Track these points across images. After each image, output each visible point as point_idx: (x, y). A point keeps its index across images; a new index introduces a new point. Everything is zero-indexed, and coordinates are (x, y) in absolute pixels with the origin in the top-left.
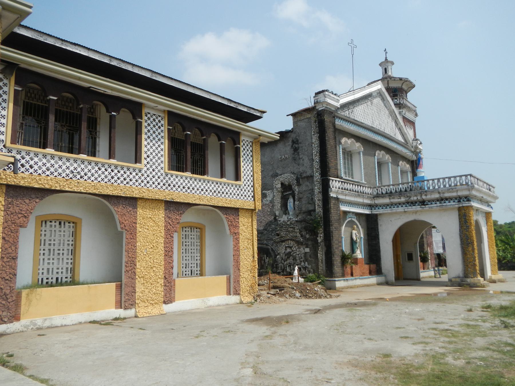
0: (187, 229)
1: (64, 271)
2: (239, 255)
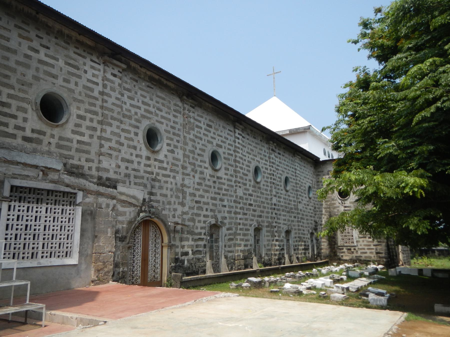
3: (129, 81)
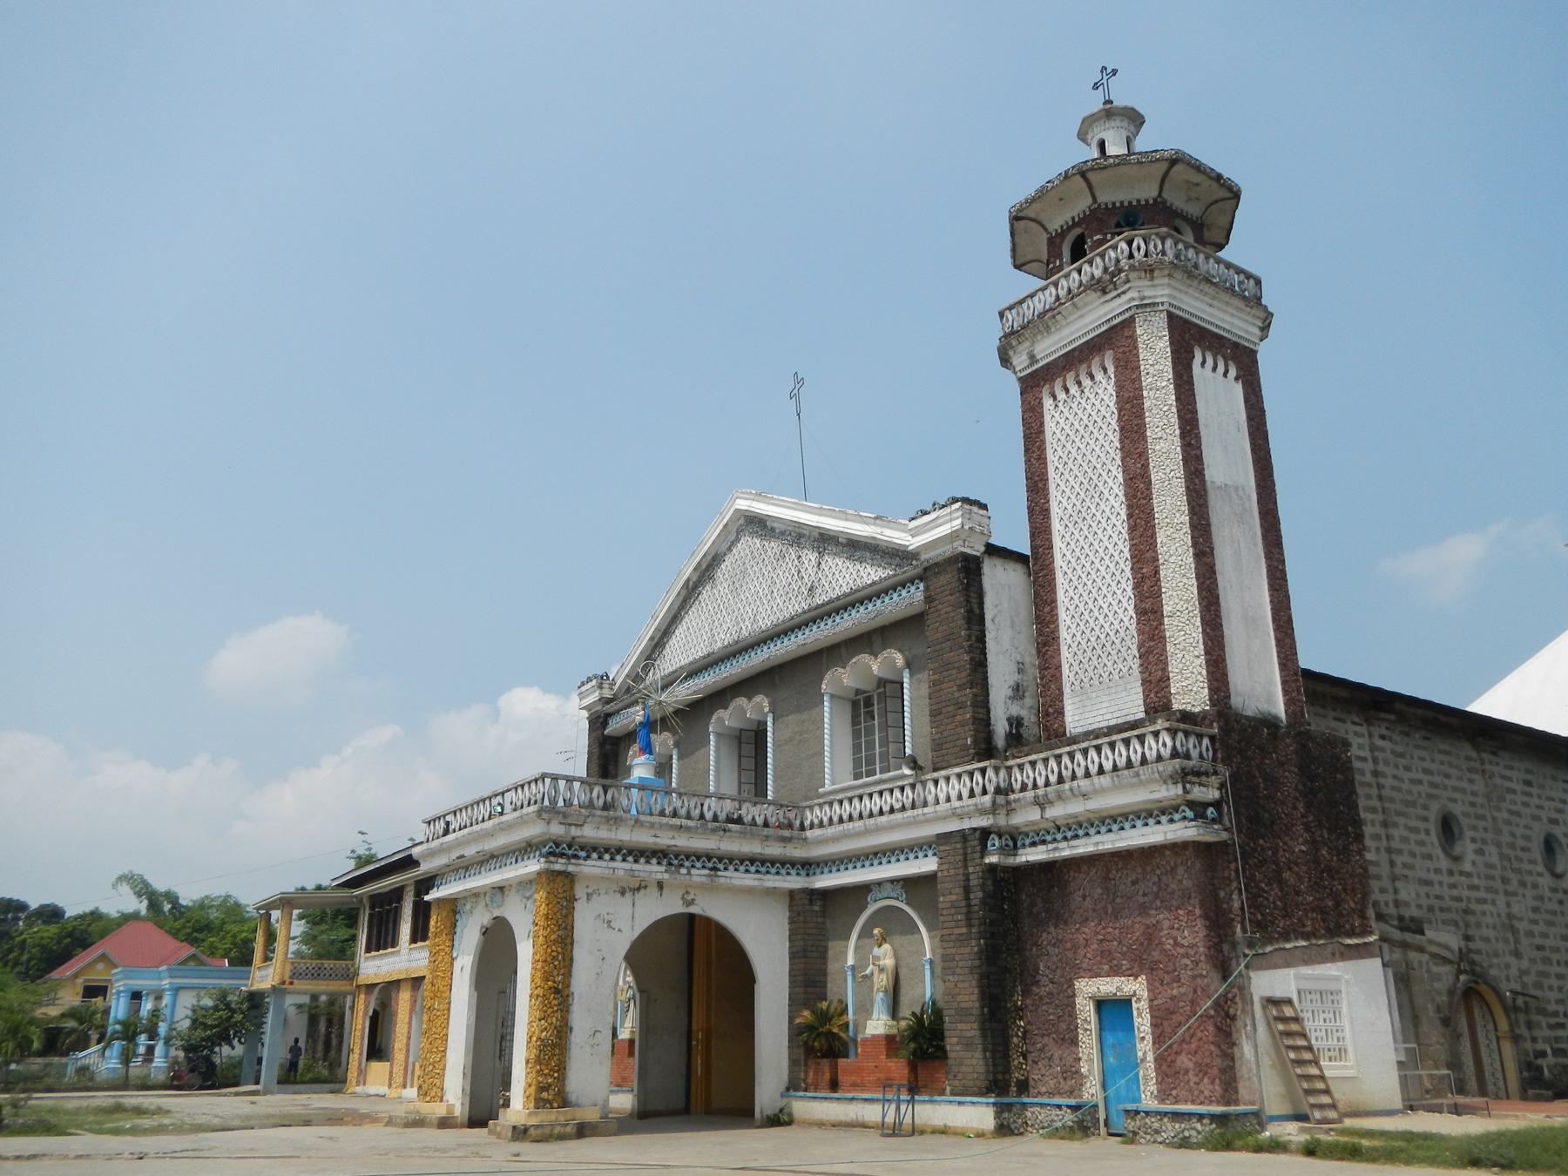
3: (1399, 738)
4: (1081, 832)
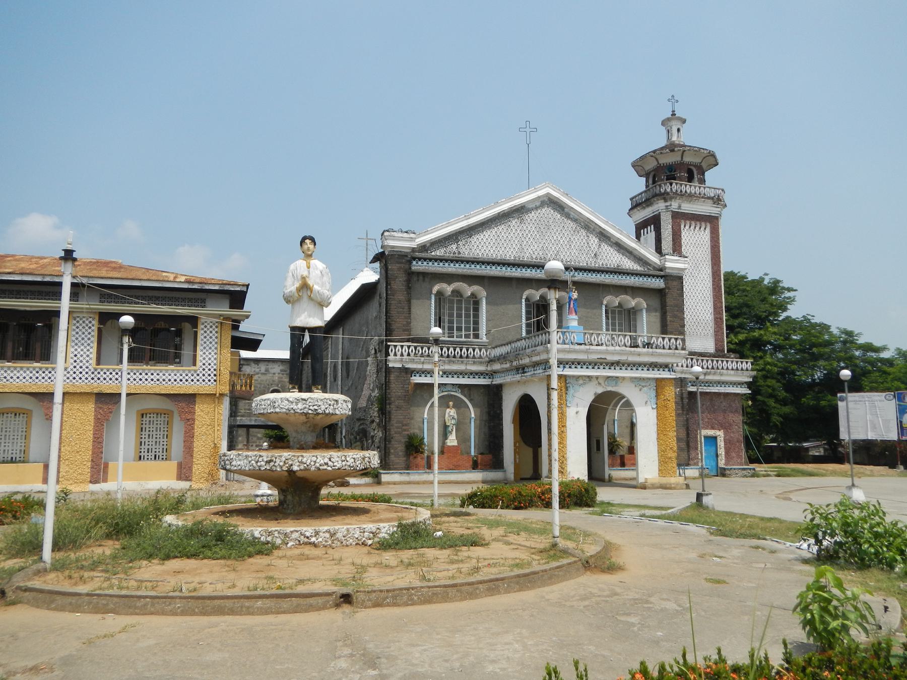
0: (152, 415)
1: (18, 452)
2: (192, 442)
4: (711, 385)
